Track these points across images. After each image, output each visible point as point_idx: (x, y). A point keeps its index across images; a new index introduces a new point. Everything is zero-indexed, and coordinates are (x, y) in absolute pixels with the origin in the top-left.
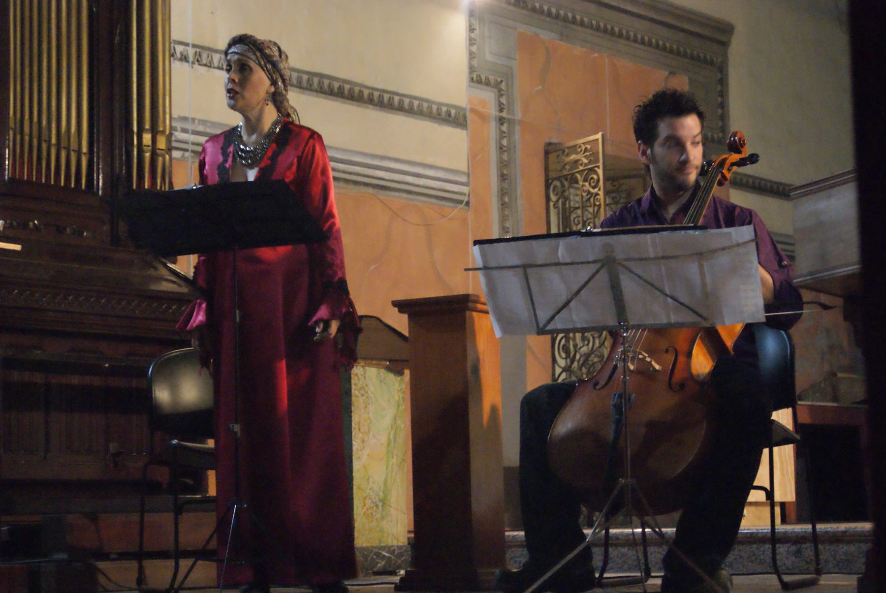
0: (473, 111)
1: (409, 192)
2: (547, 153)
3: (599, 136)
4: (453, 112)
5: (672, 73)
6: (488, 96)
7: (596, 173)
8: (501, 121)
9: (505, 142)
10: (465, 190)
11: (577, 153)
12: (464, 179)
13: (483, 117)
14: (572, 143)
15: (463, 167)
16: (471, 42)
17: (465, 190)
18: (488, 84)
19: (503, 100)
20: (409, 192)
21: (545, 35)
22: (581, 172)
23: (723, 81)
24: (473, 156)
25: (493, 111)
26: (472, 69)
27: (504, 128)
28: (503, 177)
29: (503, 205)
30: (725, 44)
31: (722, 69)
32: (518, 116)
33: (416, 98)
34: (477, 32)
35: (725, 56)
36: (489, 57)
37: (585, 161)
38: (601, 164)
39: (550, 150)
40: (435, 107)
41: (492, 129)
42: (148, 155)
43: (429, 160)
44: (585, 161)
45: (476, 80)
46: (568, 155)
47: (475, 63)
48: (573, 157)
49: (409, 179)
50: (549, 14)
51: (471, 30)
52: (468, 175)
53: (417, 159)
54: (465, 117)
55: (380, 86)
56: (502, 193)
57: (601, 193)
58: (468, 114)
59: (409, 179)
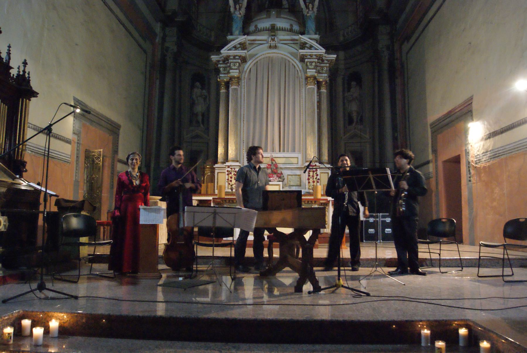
0: (73, 140)
1: (58, 159)
2: (86, 151)
3: (102, 150)
4: (69, 140)
5: (110, 135)
6: (76, 137)
7: (100, 158)
8: (78, 143)
9: (78, 148)
10: (70, 159)
11: (95, 153)
12: (70, 157)
13: (75, 142)
14: (93, 151)
15: (69, 154)
16: (74, 124)
17: (70, 159)
18: (76, 134)
19: (79, 138)
20: (58, 159)
21: (88, 124)
22: (95, 158)
23: (118, 138)
24: (72, 151)
25: (76, 141)
26: (73, 130)
27: (78, 145)
28: (77, 157)
29: (77, 164)
30: (119, 130)
31: (118, 135)
32: (81, 143)
33: (62, 136)
34: (75, 121)
35: (119, 132)
36: (77, 128)
37: (97, 155)
38: (102, 156)
39: (86, 151)
40: (65, 139)
41: (76, 144)
42: (20, 150)
43: (63, 152)
44: (97, 155)
45: (74, 133)
46: (92, 153)
47: (74, 129)
48: (93, 154)
49: (59, 156)
50: (89, 119)
51: (74, 121)
52: (71, 156)
53: (61, 151)
54: (71, 142)
55: (55, 133)
56: (77, 161)
57: (101, 163)
58: (72, 141)
59: (59, 156)
